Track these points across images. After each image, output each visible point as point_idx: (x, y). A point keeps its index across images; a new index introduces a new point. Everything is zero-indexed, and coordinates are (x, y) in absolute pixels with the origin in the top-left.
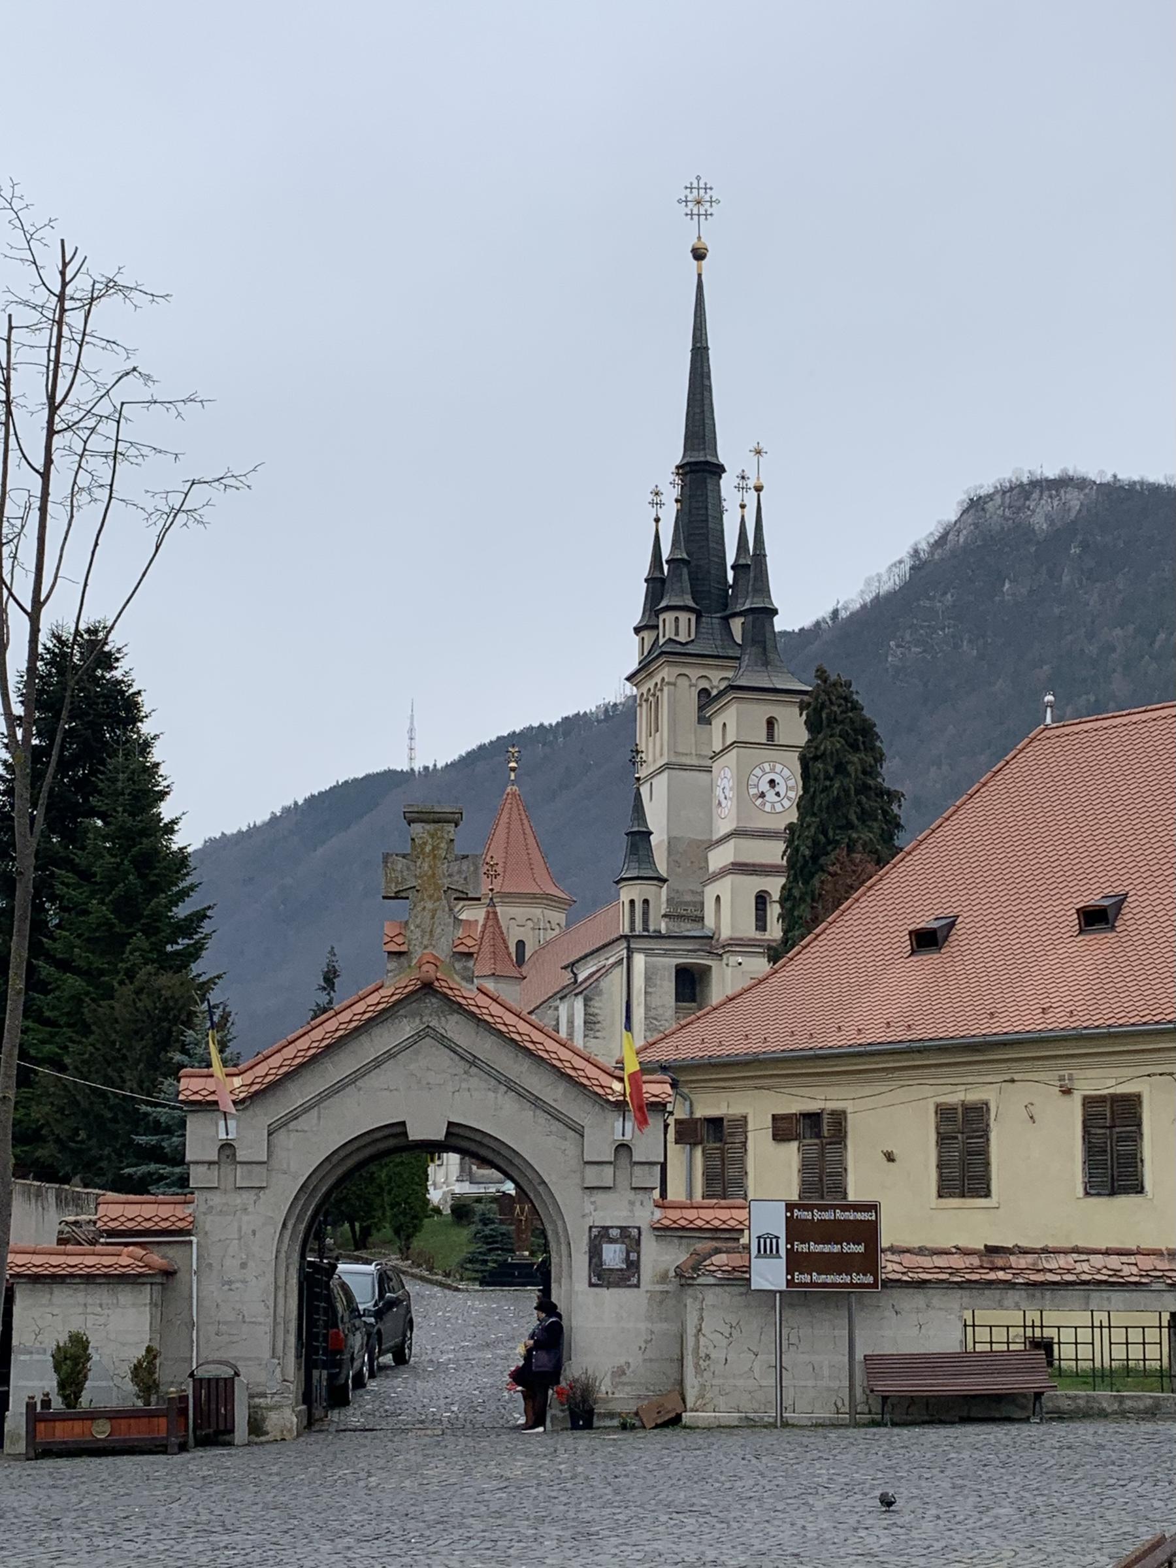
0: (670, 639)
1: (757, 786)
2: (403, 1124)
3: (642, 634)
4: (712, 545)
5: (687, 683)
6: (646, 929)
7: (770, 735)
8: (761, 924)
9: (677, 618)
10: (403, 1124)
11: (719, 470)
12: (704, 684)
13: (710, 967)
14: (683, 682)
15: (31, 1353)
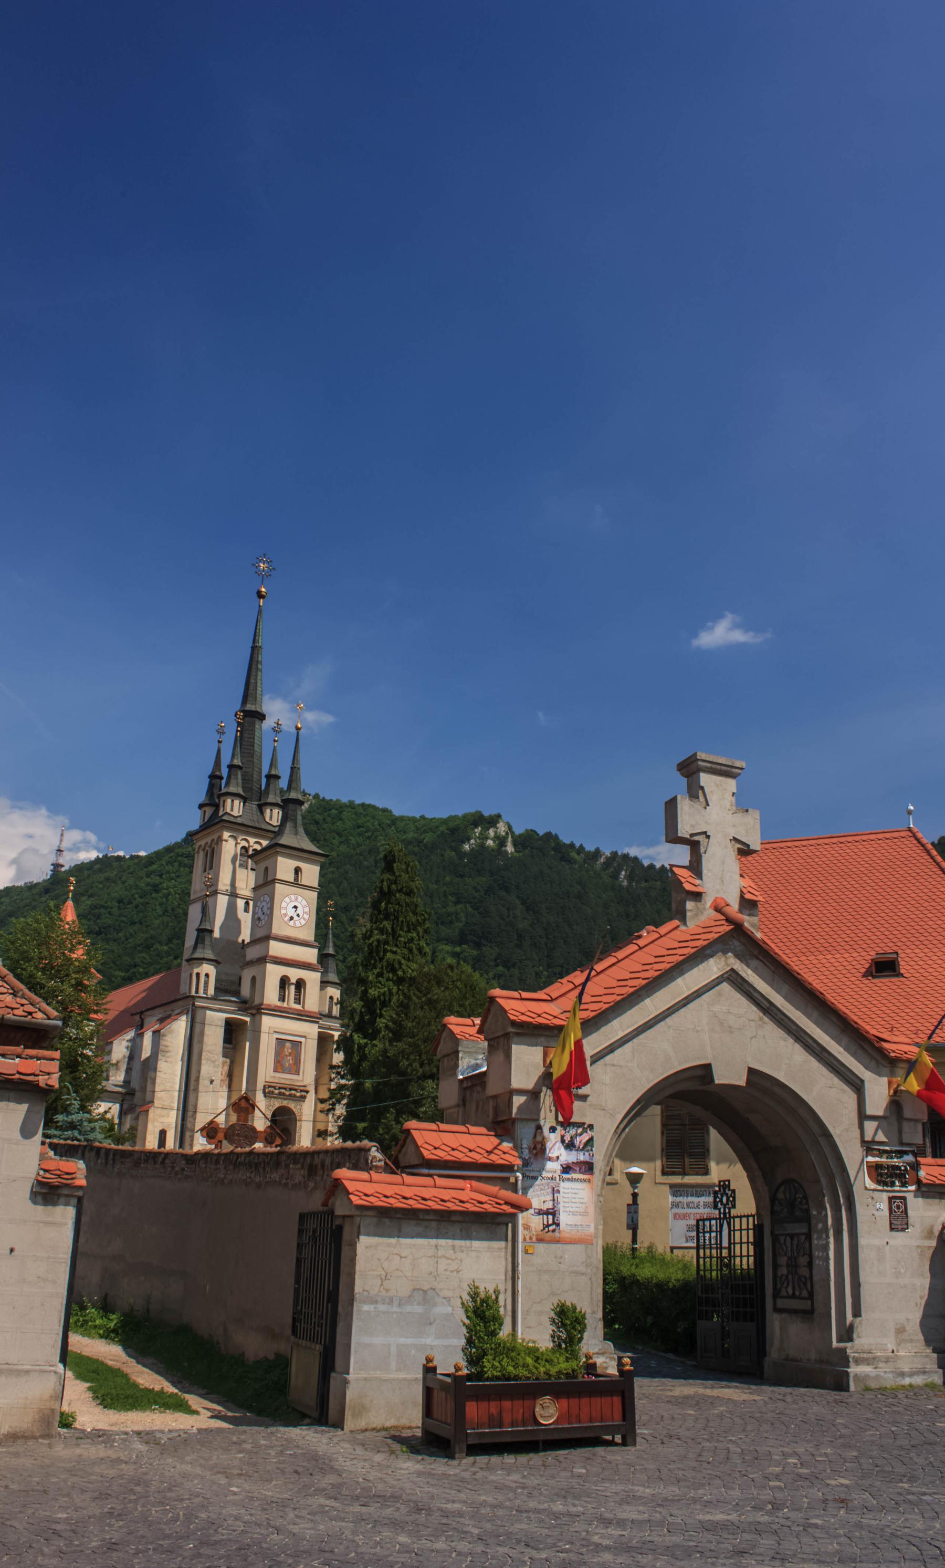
0: (227, 813)
1: (286, 908)
2: (707, 1067)
3: (204, 809)
4: (255, 760)
6: (206, 991)
7: (296, 879)
8: (282, 998)
10: (707, 1067)
11: (262, 717)
12: (244, 844)
14: (232, 842)
15: (376, 1302)
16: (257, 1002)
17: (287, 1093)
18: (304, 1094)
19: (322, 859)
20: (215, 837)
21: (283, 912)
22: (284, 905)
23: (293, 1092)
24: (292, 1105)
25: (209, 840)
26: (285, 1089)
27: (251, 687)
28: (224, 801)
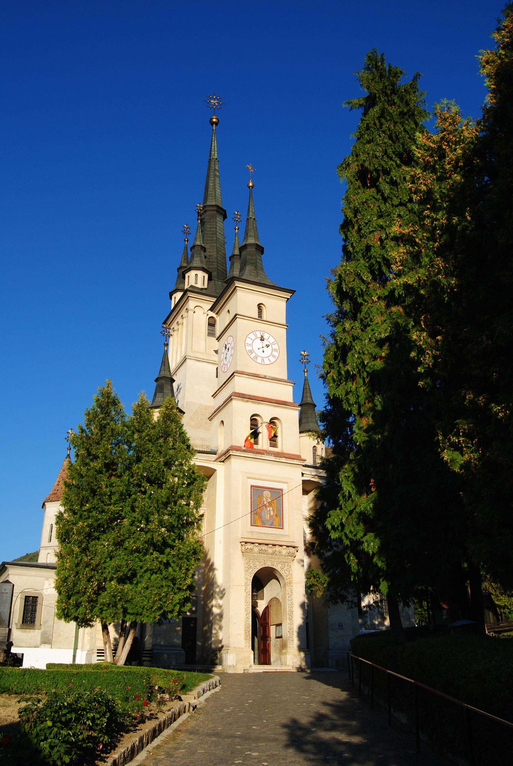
0: (191, 286)
1: (251, 345)
3: (173, 297)
13: (214, 471)
18: (292, 550)
19: (288, 295)
20: (183, 312)
21: (248, 348)
22: (248, 341)
23: (277, 548)
24: (278, 567)
27: (210, 189)
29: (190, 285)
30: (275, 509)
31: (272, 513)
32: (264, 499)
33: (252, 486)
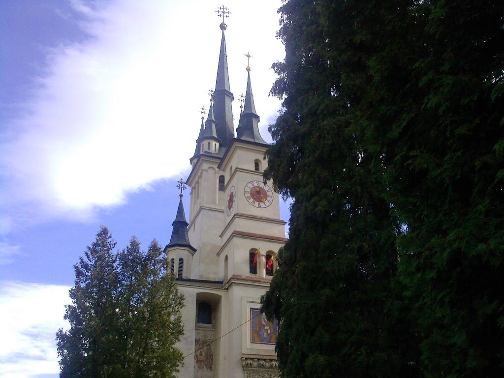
0: (206, 152)
3: (193, 163)
5: (214, 172)
8: (253, 269)
9: (209, 143)
13: (219, 298)
14: (211, 172)
16: (229, 277)
17: (268, 365)
20: (199, 174)
25: (196, 180)
26: (265, 360)
28: (203, 145)
29: (204, 151)
30: (272, 328)
31: (269, 332)
32: (262, 320)
33: (251, 309)
